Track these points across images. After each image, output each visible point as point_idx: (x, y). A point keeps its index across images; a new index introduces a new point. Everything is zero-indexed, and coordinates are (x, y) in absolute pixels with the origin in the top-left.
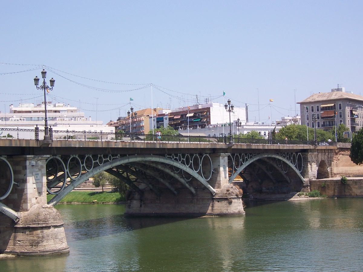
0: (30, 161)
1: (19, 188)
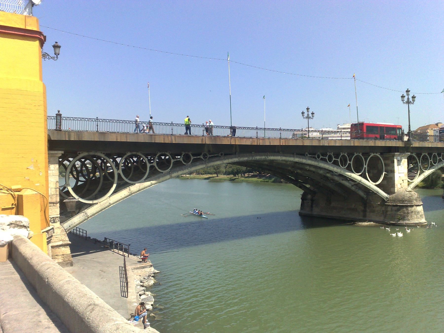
0: (397, 157)
1: (388, 176)
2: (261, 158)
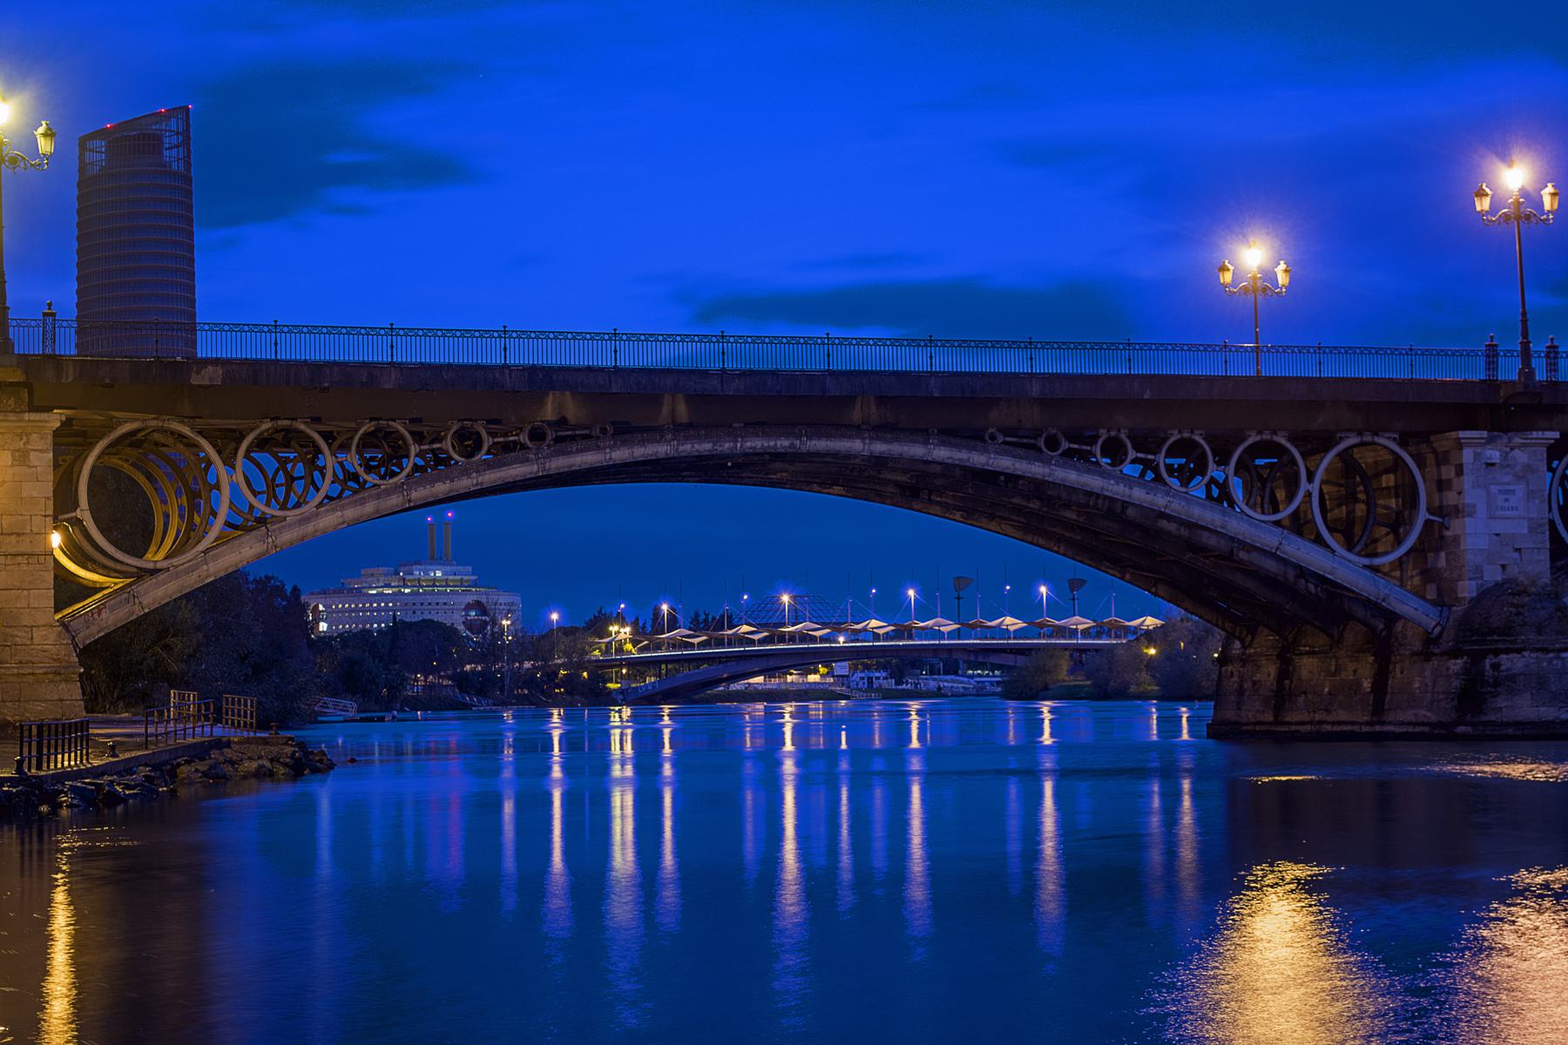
2: (772, 444)
